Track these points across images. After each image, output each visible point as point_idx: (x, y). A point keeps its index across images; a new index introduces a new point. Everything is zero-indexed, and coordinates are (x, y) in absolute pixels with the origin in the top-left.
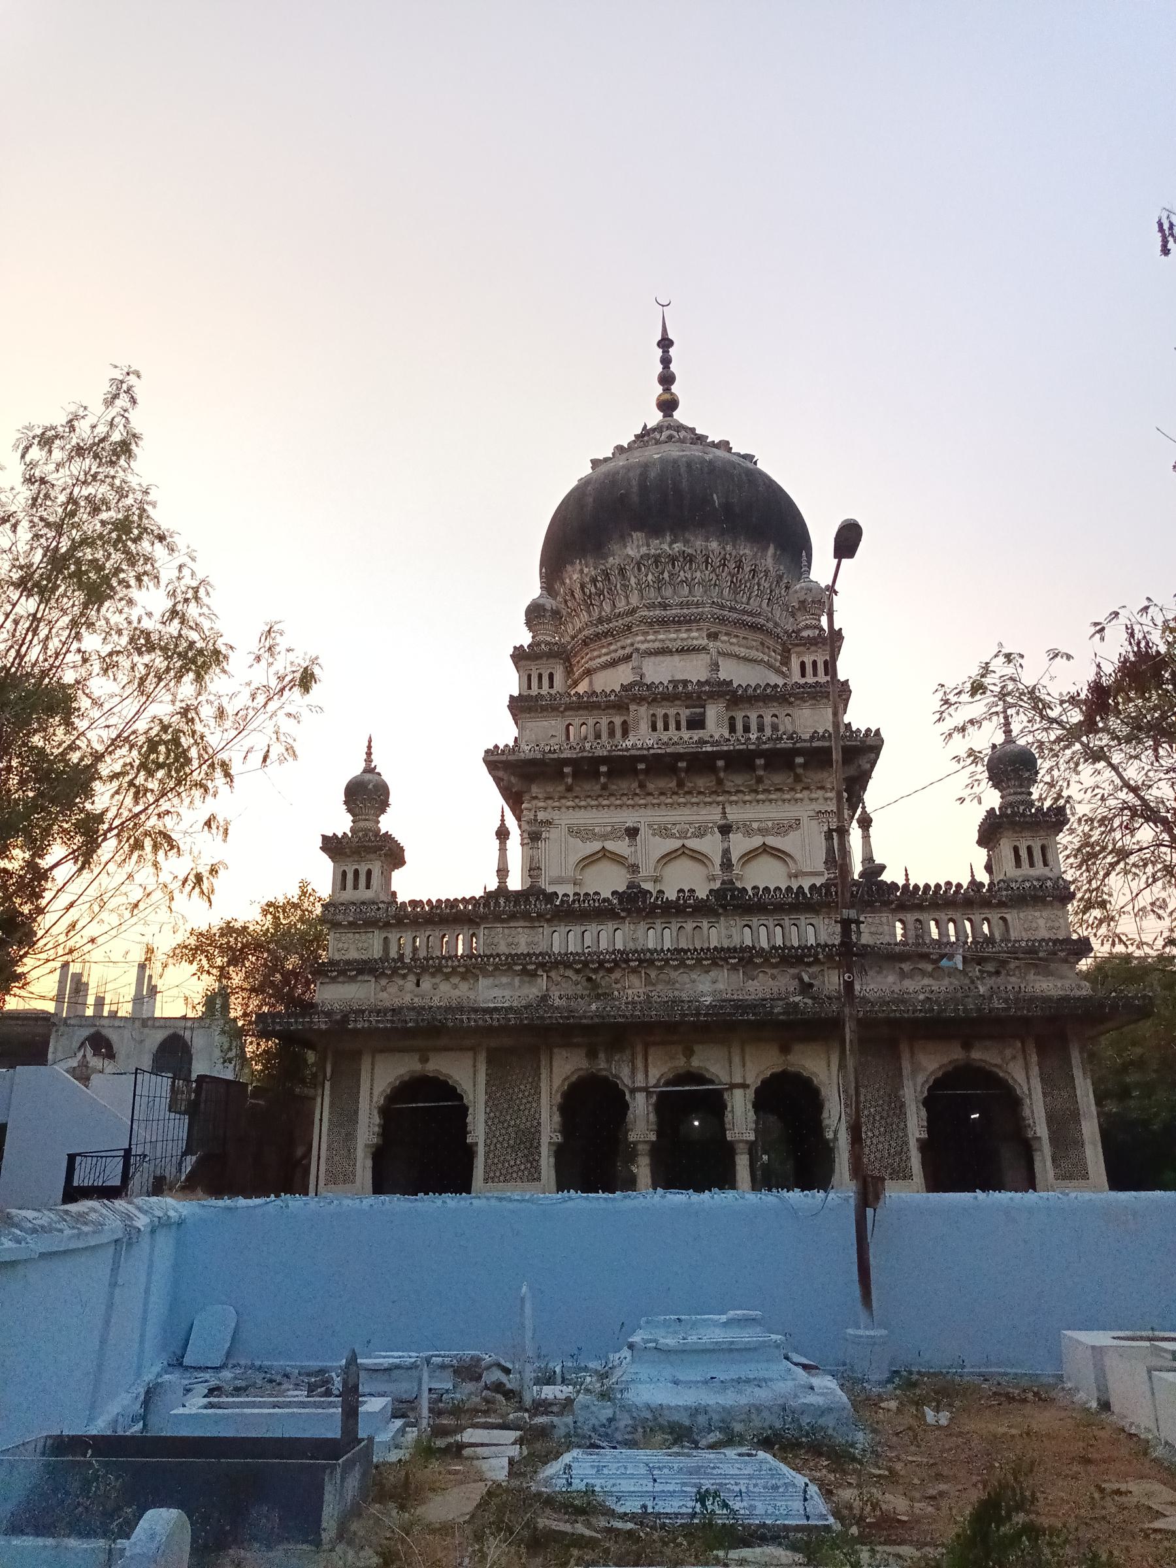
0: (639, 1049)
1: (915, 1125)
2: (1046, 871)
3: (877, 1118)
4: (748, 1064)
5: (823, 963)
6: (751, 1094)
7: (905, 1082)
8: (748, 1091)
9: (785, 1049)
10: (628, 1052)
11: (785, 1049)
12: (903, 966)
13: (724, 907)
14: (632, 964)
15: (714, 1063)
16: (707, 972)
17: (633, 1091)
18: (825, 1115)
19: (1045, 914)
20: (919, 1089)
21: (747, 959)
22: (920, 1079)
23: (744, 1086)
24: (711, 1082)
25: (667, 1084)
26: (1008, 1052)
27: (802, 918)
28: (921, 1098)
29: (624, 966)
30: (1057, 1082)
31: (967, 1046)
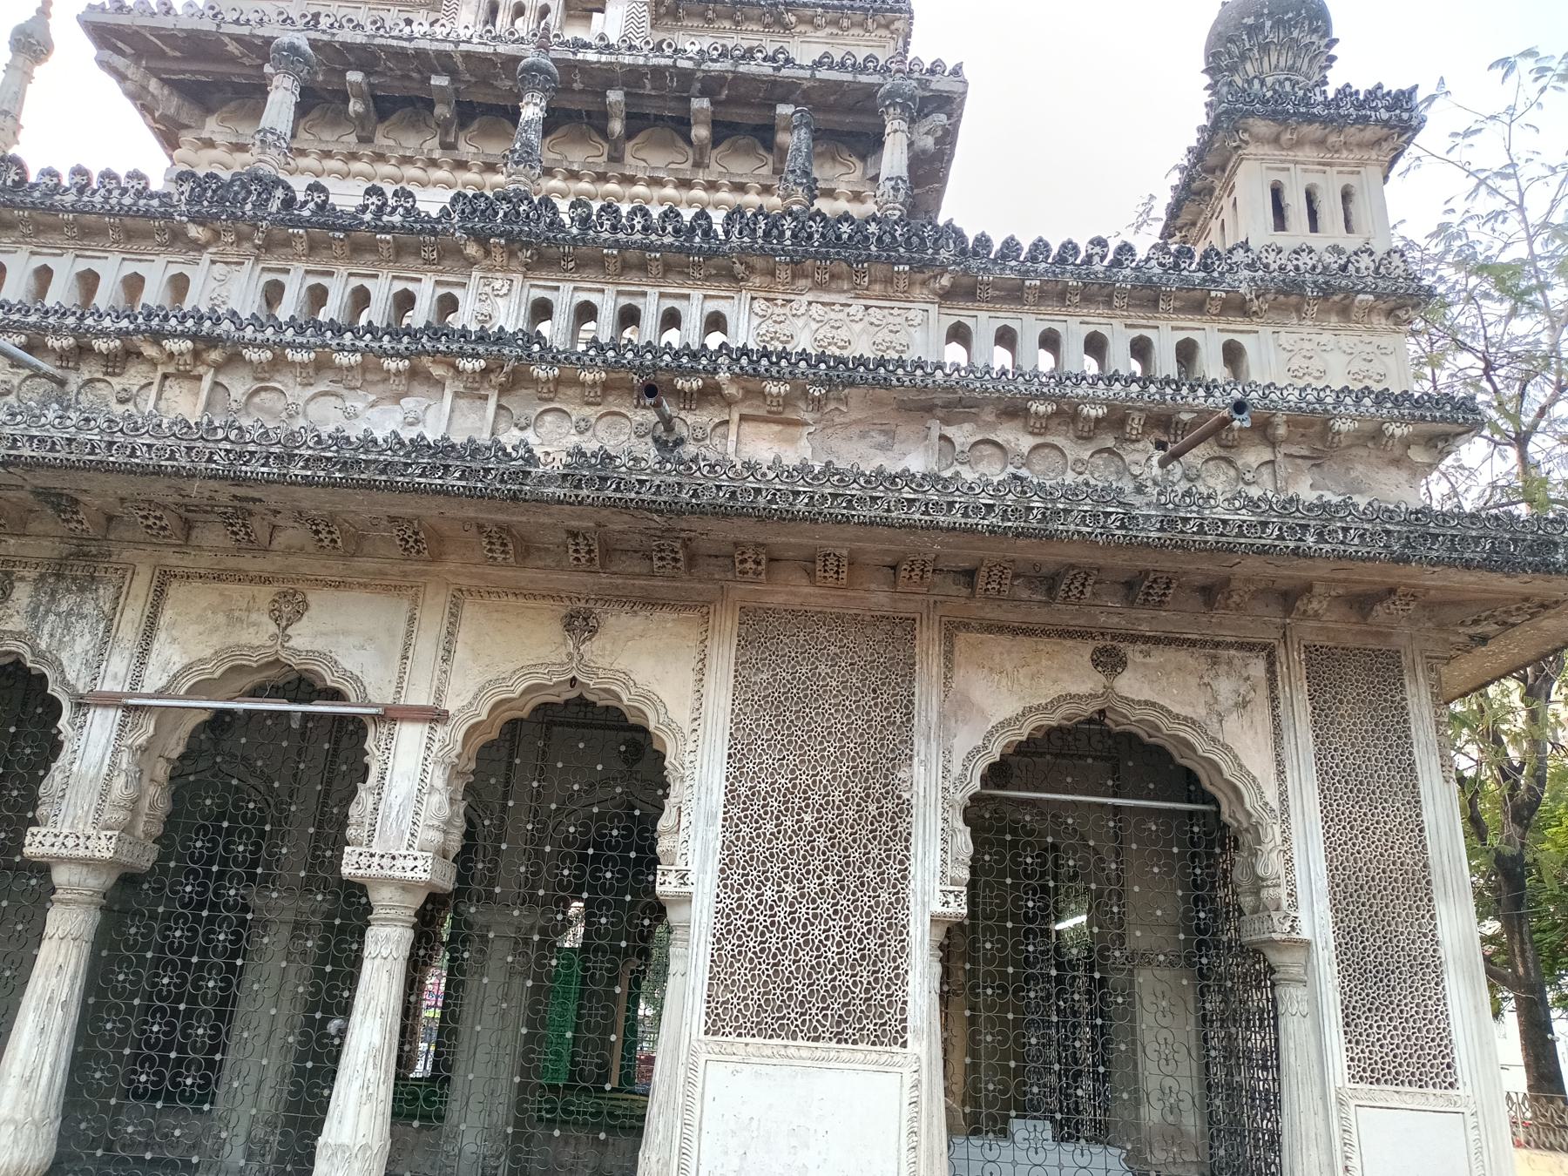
0: (141, 586)
1: (934, 877)
2: (1351, 243)
3: (821, 842)
4: (461, 653)
5: (729, 403)
6: (451, 736)
7: (919, 743)
8: (441, 732)
9: (580, 624)
10: (105, 593)
11: (580, 624)
12: (950, 431)
13: (481, 239)
14: (172, 345)
15: (356, 645)
16: (397, 398)
17: (81, 704)
18: (664, 823)
19: (1346, 340)
20: (956, 769)
21: (509, 368)
22: (966, 739)
23: (434, 716)
24: (336, 695)
25: (192, 692)
26: (1225, 687)
27: (697, 295)
28: (961, 797)
29: (150, 351)
30: (1367, 784)
31: (1109, 661)
